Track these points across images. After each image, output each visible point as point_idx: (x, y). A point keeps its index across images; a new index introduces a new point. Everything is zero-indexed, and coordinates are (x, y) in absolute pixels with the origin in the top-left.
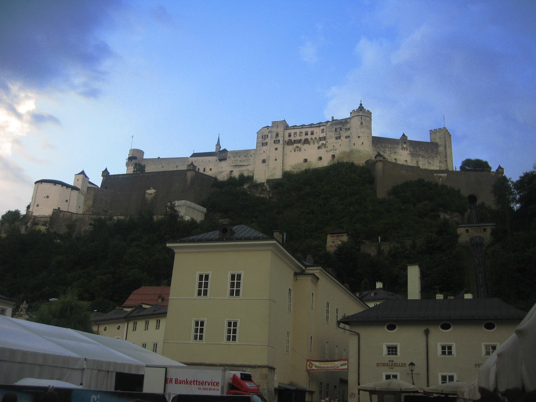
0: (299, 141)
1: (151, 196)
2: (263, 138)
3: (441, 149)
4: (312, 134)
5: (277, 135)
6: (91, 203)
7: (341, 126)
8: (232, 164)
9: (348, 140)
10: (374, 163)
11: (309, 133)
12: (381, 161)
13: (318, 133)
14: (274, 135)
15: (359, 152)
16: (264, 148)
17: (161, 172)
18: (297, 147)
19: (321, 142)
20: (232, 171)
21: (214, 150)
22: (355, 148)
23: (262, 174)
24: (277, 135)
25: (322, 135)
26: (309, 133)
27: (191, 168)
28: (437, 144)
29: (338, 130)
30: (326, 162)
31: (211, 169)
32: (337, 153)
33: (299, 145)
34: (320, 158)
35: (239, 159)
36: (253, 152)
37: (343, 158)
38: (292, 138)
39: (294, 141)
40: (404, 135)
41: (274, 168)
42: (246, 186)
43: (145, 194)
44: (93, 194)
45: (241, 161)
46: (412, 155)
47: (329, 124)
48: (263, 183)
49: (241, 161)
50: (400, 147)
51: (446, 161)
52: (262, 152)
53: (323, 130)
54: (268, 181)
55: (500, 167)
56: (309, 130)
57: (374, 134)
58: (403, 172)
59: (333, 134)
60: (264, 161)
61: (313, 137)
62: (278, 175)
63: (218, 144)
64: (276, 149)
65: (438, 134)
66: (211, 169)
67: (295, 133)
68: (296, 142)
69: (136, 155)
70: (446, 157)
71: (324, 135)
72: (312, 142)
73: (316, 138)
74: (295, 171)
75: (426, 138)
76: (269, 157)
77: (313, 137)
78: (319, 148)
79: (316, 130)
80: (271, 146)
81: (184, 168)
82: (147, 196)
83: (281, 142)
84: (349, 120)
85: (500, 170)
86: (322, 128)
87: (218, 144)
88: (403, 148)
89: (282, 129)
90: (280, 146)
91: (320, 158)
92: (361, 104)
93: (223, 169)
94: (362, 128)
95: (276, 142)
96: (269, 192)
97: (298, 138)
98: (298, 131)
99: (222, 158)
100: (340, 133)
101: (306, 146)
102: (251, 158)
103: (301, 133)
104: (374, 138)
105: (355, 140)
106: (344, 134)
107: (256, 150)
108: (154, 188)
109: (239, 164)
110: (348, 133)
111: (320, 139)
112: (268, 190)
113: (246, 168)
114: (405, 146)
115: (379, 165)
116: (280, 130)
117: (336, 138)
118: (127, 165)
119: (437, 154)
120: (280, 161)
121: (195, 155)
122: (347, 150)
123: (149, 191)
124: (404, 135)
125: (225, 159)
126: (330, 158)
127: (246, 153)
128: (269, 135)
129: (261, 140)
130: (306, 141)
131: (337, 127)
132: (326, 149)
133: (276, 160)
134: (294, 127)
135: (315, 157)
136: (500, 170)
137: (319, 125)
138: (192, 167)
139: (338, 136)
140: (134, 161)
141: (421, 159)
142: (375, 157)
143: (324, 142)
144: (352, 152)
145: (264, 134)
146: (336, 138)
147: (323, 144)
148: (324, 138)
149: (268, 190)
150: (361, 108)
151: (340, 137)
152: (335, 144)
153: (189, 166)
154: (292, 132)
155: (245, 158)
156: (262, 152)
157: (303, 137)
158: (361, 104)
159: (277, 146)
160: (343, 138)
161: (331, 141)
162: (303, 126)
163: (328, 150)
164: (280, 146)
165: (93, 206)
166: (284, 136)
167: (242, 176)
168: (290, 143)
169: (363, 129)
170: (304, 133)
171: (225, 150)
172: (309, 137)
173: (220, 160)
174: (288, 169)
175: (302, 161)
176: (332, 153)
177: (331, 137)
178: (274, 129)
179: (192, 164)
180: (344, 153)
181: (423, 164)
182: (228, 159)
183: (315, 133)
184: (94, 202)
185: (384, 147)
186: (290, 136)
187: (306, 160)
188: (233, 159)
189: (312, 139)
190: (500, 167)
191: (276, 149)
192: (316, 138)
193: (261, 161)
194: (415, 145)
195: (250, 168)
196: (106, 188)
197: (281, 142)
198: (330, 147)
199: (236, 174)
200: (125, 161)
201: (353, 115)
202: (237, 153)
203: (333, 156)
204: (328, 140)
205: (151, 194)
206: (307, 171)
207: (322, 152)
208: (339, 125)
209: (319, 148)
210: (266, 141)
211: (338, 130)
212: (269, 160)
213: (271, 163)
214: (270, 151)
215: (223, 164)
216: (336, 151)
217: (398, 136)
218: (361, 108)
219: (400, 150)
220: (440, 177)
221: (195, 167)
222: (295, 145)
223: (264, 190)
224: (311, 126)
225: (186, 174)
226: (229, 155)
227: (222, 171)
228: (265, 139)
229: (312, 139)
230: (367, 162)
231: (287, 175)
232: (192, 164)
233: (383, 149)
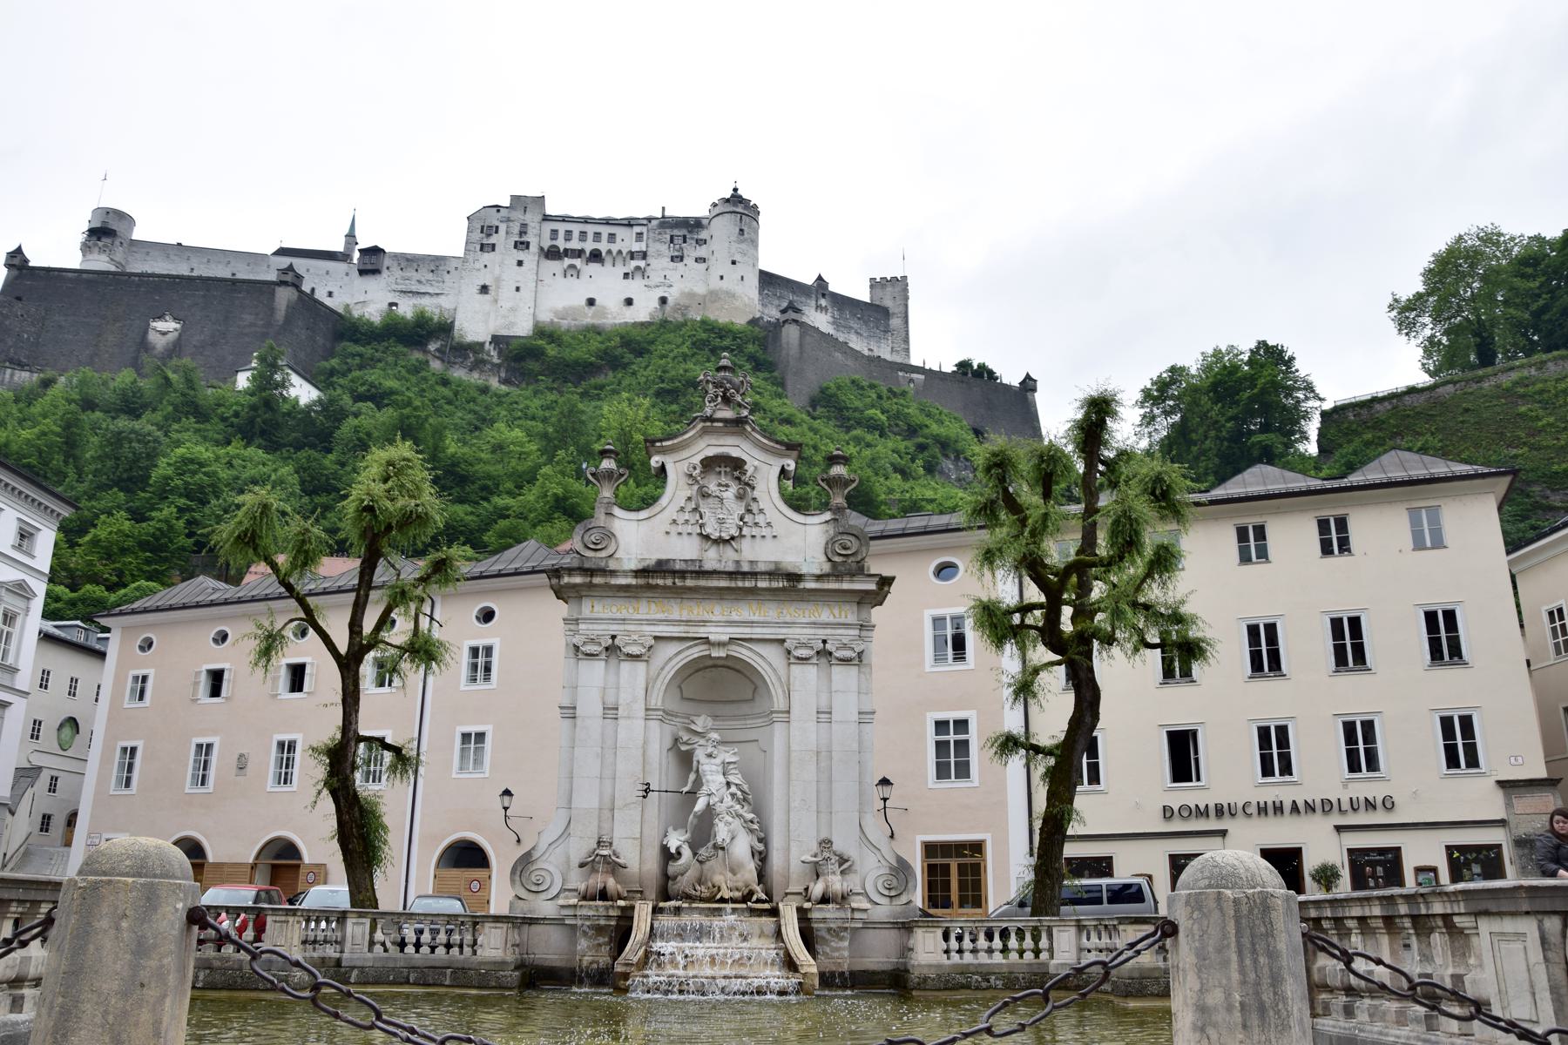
0: (579, 253)
2: (482, 230)
3: (895, 322)
4: (612, 237)
5: (522, 233)
9: (703, 266)
10: (777, 326)
11: (605, 237)
12: (796, 321)
13: (627, 241)
14: (516, 229)
15: (731, 295)
18: (572, 266)
19: (634, 263)
20: (391, 304)
21: (338, 246)
22: (724, 285)
23: (475, 325)
24: (522, 233)
25: (636, 247)
26: (605, 237)
27: (289, 278)
28: (884, 309)
29: (678, 241)
30: (644, 310)
31: (330, 294)
32: (673, 295)
33: (577, 262)
34: (629, 302)
36: (454, 264)
37: (687, 307)
38: (561, 244)
39: (566, 250)
40: (820, 278)
41: (513, 310)
42: (432, 347)
43: (146, 333)
46: (835, 323)
47: (654, 223)
48: (482, 344)
50: (813, 303)
51: (907, 350)
52: (479, 265)
53: (640, 235)
54: (497, 340)
55: (1028, 377)
56: (605, 231)
57: (769, 263)
58: (838, 355)
59: (664, 248)
60: (484, 289)
62: (522, 328)
63: (351, 237)
64: (520, 263)
65: (889, 289)
66: (330, 294)
67: (569, 233)
68: (567, 253)
69: (114, 225)
70: (906, 340)
72: (608, 260)
73: (620, 252)
74: (565, 323)
75: (864, 296)
76: (498, 280)
77: (615, 250)
78: (626, 275)
79: (621, 232)
80: (505, 254)
81: (272, 276)
82: (152, 337)
83: (534, 248)
84: (705, 222)
85: (1029, 384)
86: (637, 229)
87: (351, 237)
88: (818, 307)
89: (540, 217)
90: (530, 257)
91: (629, 302)
92: (735, 190)
93: (368, 297)
94: (742, 242)
95: (522, 245)
96: (499, 366)
97: (575, 244)
98: (576, 229)
99: (369, 267)
101: (594, 267)
102: (447, 277)
103: (583, 234)
104: (762, 272)
105: (720, 265)
106: (692, 252)
107: (464, 260)
108: (175, 319)
109: (414, 288)
110: (702, 251)
111: (632, 255)
112: (496, 360)
113: (435, 300)
114: (823, 302)
115: (791, 334)
116: (532, 219)
118: (86, 248)
119: (886, 332)
120: (527, 293)
121: (282, 252)
122: (700, 289)
123: (160, 325)
124: (820, 278)
125: (376, 272)
126: (655, 304)
127: (436, 264)
128: (503, 227)
129: (477, 235)
130: (596, 256)
131: (676, 232)
132: (646, 282)
133: (518, 289)
134: (564, 219)
135: (616, 298)
136: (1029, 384)
137: (629, 223)
138: (291, 279)
140: (106, 240)
141: (853, 337)
142: (783, 312)
143: (642, 264)
144: (714, 296)
147: (638, 268)
148: (644, 255)
149: (496, 360)
150: (736, 199)
153: (285, 271)
154: (562, 228)
156: (479, 265)
157: (589, 246)
158: (735, 190)
159: (521, 255)
160: (689, 261)
161: (660, 265)
162: (586, 221)
164: (530, 257)
166: (539, 237)
168: (552, 254)
169: (743, 246)
170: (590, 236)
171: (375, 251)
172: (603, 246)
173: (362, 272)
174: (545, 317)
175: (583, 302)
176: (660, 293)
177: (659, 255)
178: (517, 215)
179: (291, 268)
180: (691, 295)
182: (385, 273)
183: (618, 239)
186: (554, 232)
187: (591, 302)
189: (609, 252)
190: (1028, 377)
191: (520, 263)
192: (620, 252)
193: (475, 289)
194: (843, 304)
195: (446, 303)
196: (19, 299)
197: (534, 248)
198: (656, 277)
199: (406, 309)
200: (81, 238)
201: (717, 210)
202: (409, 261)
203: (663, 300)
204: (650, 260)
205: (164, 334)
206: (596, 330)
207: (634, 288)
208: (683, 231)
209: (626, 275)
210: (492, 240)
211: (678, 241)
212: (498, 287)
213: (506, 295)
214: (501, 264)
215: (371, 283)
217: (809, 279)
218: (736, 199)
220: (911, 380)
221: (299, 277)
222: (567, 261)
223: (484, 362)
224: (607, 222)
225: (273, 294)
226: (387, 262)
227: (369, 301)
228: (489, 235)
229: (609, 252)
230: (754, 322)
231: (541, 332)
232: (291, 268)
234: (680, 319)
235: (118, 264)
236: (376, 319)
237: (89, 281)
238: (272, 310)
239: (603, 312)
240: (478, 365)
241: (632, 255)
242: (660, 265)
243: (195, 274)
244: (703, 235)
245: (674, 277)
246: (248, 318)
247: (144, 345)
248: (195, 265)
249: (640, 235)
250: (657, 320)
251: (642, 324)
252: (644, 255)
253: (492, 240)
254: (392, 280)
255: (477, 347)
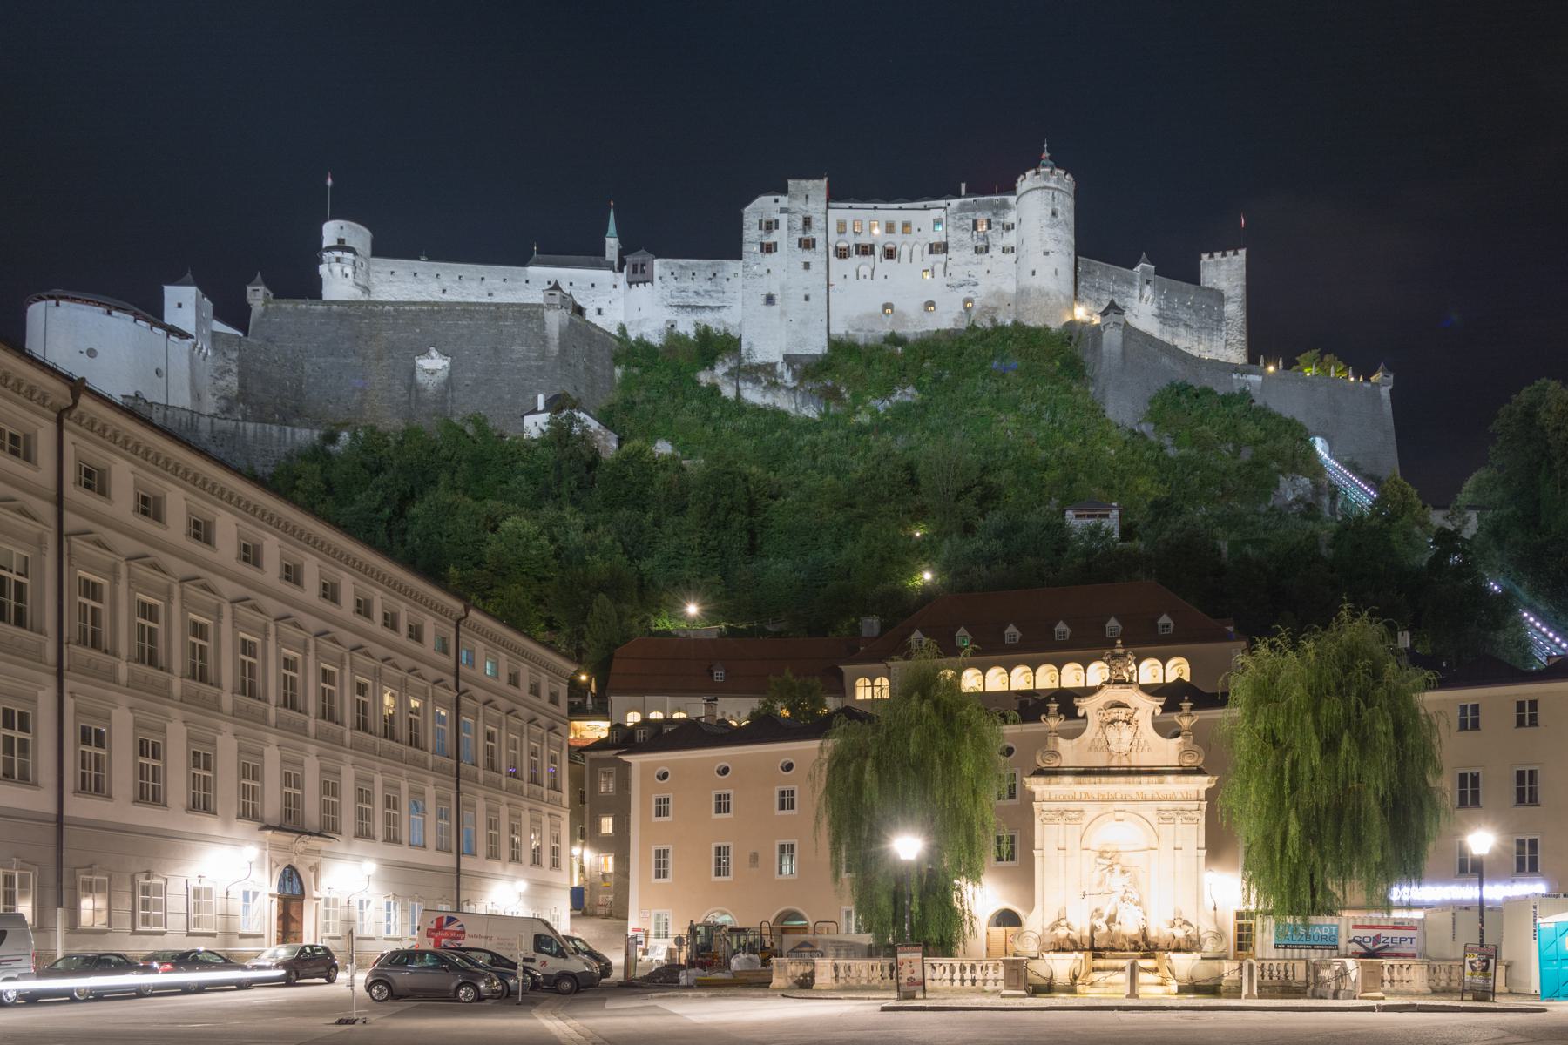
1: (435, 379)
6: (235, 387)
7: (989, 215)
8: (670, 301)
9: (1012, 257)
11: (898, 227)
14: (799, 224)
16: (769, 258)
17: (459, 303)
19: (934, 257)
26: (898, 227)
30: (947, 318)
32: (980, 295)
33: (868, 259)
35: (688, 284)
37: (995, 309)
38: (849, 241)
39: (857, 246)
41: (804, 323)
42: (720, 370)
43: (413, 372)
44: (235, 355)
45: (697, 293)
48: (774, 365)
49: (697, 293)
54: (789, 359)
59: (966, 237)
60: (770, 300)
61: (910, 238)
62: (816, 345)
64: (807, 266)
71: (938, 235)
82: (421, 377)
90: (816, 257)
95: (807, 244)
96: (795, 388)
100: (986, 237)
105: (1034, 259)
109: (693, 301)
110: (1010, 239)
111: (934, 248)
112: (791, 383)
117: (977, 250)
120: (818, 301)
123: (424, 363)
130: (890, 254)
132: (947, 280)
133: (807, 298)
139: (980, 244)
143: (942, 257)
145: (765, 218)
146: (977, 250)
151: (987, 249)
152: (973, 269)
155: (708, 286)
159: (807, 256)
160: (995, 252)
161: (962, 258)
163: (952, 282)
165: (244, 394)
167: (704, 334)
168: (843, 254)
172: (896, 239)
174: (838, 329)
176: (964, 293)
180: (1000, 295)
181: (1185, 341)
183: (914, 228)
184: (242, 386)
185: (1098, 290)
186: (842, 228)
187: (887, 306)
188: (673, 284)
191: (807, 266)
193: (760, 301)
197: (820, 246)
199: (686, 326)
204: (951, 253)
205: (433, 373)
210: (774, 237)
216: (976, 289)
219: (1136, 301)
225: (543, 318)
231: (836, 345)
232: (556, 287)
233: (1095, 295)
234: (988, 325)
235: (366, 290)
236: (656, 340)
237: (341, 315)
238: (545, 339)
239: (901, 318)
240: (774, 386)
241: (934, 248)
242: (962, 258)
243: (447, 297)
244: (1011, 218)
245: (978, 272)
246: (519, 349)
247: (412, 385)
248: (446, 284)
249: (937, 222)
250: (963, 326)
251: (947, 332)
252: (941, 248)
253: (774, 237)
254: (666, 292)
255: (769, 368)
